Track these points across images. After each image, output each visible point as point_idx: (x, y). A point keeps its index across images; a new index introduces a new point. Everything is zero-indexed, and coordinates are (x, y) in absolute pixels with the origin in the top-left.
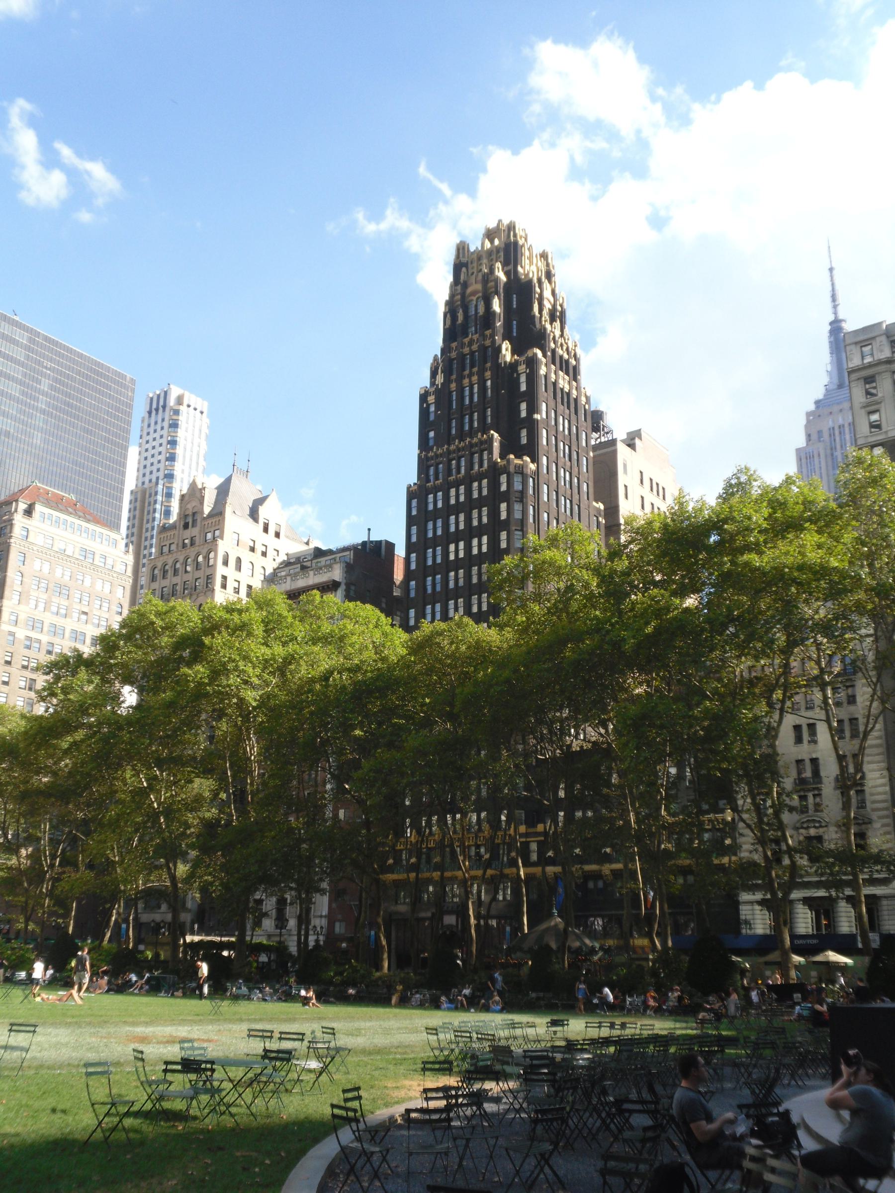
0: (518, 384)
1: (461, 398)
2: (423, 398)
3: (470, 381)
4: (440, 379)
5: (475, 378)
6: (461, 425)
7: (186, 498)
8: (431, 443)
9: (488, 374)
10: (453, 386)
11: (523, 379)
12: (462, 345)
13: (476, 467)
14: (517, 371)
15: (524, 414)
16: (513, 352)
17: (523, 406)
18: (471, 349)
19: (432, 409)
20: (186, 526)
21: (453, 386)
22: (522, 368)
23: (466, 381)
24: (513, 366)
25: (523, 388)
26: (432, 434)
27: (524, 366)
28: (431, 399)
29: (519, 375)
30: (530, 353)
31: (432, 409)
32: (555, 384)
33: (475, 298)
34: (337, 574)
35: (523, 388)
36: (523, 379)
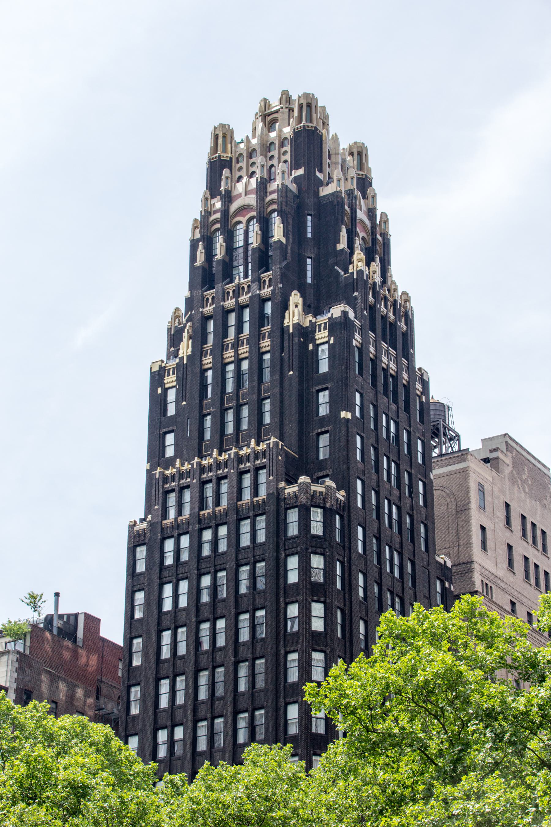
2: (157, 378)
3: (237, 354)
4: (185, 349)
12: (224, 296)
15: (323, 411)
16: (308, 308)
17: (324, 397)
18: (237, 301)
19: (172, 395)
21: (208, 361)
22: (322, 336)
23: (229, 354)
24: (306, 334)
28: (170, 380)
30: (336, 311)
31: (172, 395)
32: (375, 362)
33: (244, 220)
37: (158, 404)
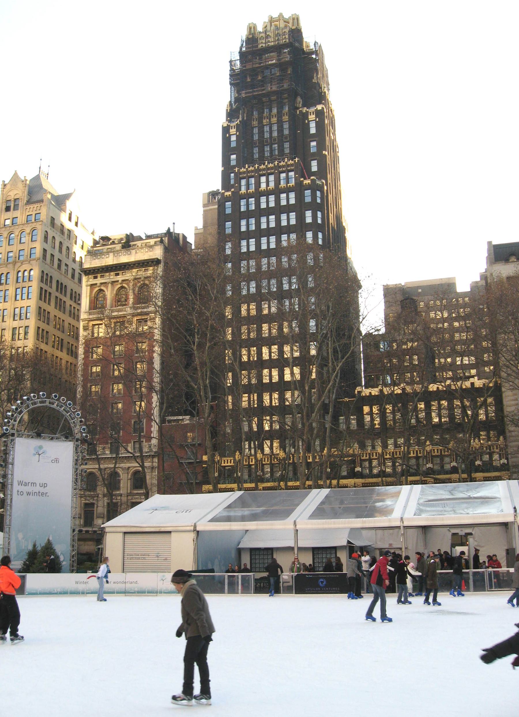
0: (309, 128)
1: (261, 132)
5: (274, 120)
6: (262, 152)
7: (8, 187)
8: (233, 163)
9: (286, 118)
10: (255, 123)
11: (313, 125)
13: (282, 182)
14: (308, 119)
19: (233, 138)
20: (8, 209)
22: (312, 117)
25: (313, 131)
26: (233, 157)
27: (314, 116)
29: (309, 121)
31: (233, 138)
34: (158, 253)
35: (313, 131)
36: (313, 125)
37: (226, 141)
